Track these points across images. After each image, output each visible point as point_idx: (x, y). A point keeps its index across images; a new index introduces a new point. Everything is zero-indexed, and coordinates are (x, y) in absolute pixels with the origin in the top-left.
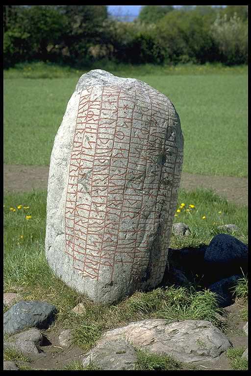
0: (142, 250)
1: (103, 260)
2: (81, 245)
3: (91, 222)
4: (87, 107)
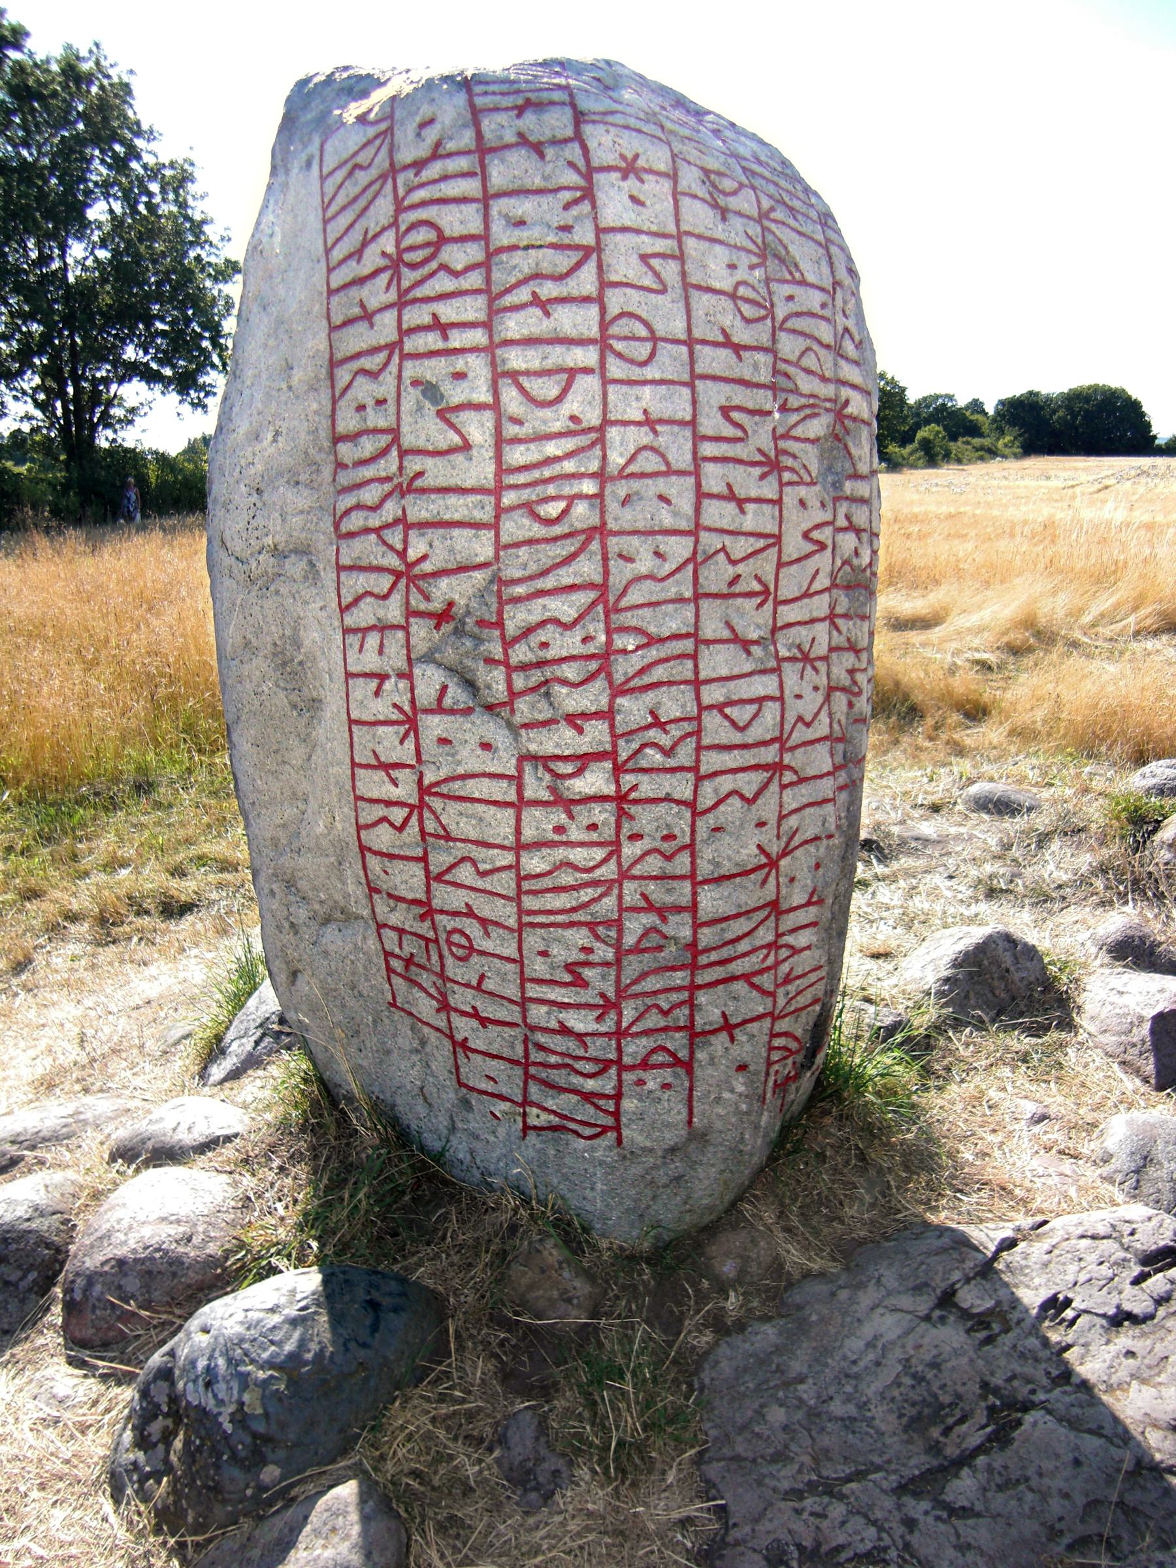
0: (802, 939)
1: (634, 1049)
2: (489, 985)
3: (534, 863)
4: (384, 208)
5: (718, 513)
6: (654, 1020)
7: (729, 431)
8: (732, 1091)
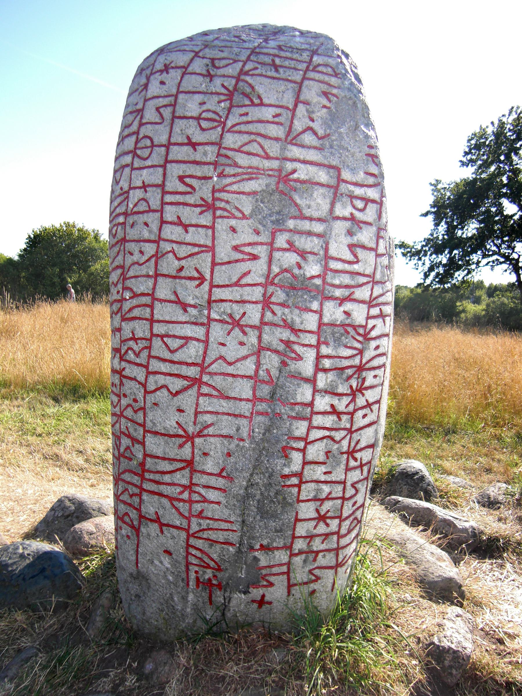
0: (212, 495)
5: (172, 232)
7: (182, 188)
8: (161, 562)
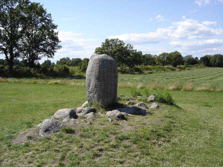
3: (101, 88)
6: (106, 95)
